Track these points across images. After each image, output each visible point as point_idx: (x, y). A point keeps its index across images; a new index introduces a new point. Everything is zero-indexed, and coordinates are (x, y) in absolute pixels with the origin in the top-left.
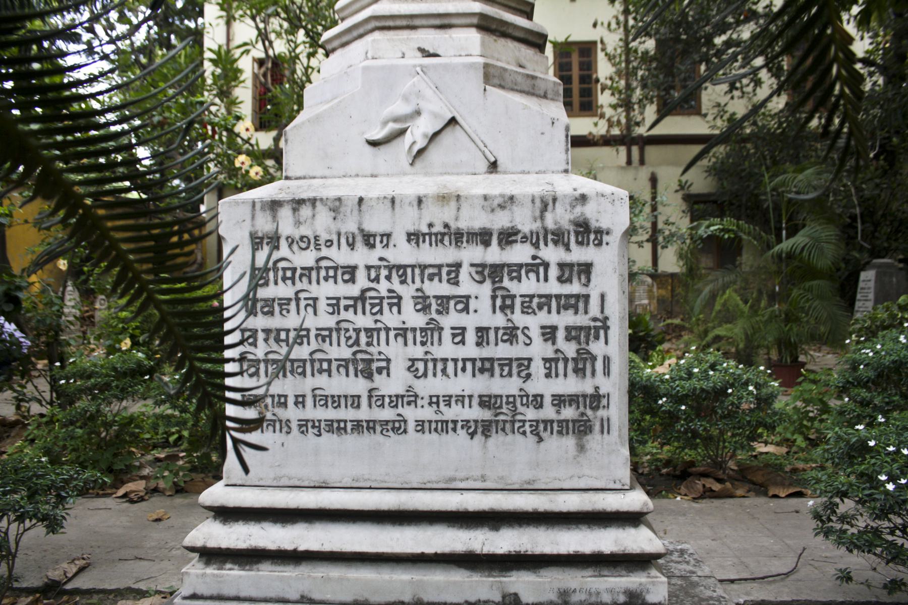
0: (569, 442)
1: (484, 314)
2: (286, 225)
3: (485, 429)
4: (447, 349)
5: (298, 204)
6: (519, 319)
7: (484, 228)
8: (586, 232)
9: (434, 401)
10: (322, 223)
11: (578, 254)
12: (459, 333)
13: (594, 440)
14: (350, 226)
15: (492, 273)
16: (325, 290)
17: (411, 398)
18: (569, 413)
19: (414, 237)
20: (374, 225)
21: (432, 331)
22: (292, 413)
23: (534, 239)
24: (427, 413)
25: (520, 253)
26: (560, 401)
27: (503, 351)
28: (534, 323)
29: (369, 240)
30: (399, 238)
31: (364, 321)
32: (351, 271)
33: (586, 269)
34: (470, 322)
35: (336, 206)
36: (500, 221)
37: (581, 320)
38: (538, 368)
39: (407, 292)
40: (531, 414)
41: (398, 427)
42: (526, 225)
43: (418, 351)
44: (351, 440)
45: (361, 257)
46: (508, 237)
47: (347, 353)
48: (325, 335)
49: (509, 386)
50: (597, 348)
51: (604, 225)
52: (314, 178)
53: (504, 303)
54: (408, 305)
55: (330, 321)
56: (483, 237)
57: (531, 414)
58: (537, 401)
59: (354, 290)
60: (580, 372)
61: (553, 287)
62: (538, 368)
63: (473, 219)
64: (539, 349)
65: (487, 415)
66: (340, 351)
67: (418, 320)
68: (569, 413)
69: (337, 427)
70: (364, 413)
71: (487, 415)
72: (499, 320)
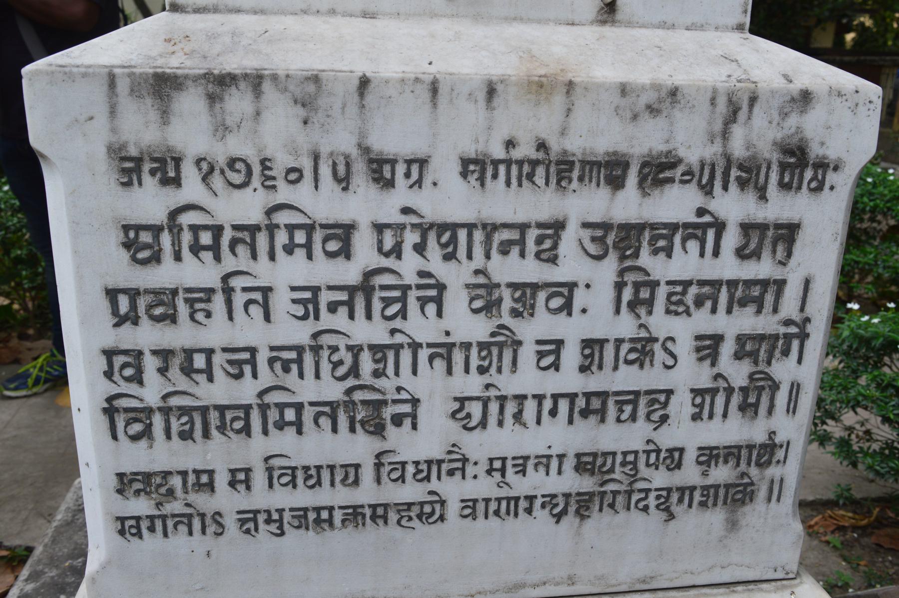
0: (716, 517)
1: (599, 314)
2: (190, 130)
3: (583, 505)
4: (527, 378)
5: (219, 84)
6: (660, 323)
7: (615, 153)
8: (800, 164)
9: (497, 467)
10: (277, 132)
11: (779, 207)
12: (551, 351)
13: (755, 514)
14: (341, 139)
15: (621, 240)
16: (288, 272)
17: (457, 464)
18: (721, 474)
19: (475, 167)
20: (391, 140)
22: (226, 500)
23: (706, 178)
24: (483, 487)
25: (676, 204)
26: (709, 456)
27: (628, 378)
28: (683, 330)
29: (381, 171)
30: (444, 168)
31: (368, 331)
32: (343, 233)
33: (788, 233)
34: (571, 330)
35: (309, 93)
36: (646, 139)
37: (766, 324)
38: (681, 406)
39: (456, 276)
40: (660, 479)
41: (430, 512)
43: (473, 385)
44: (341, 540)
45: (364, 205)
46: (658, 171)
47: (333, 391)
48: (288, 359)
50: (784, 370)
51: (832, 153)
52: (238, 11)
53: (637, 295)
54: (457, 302)
56: (611, 171)
57: (660, 479)
58: (674, 458)
59: (349, 272)
60: (748, 409)
61: (728, 267)
62: (681, 406)
63: (595, 134)
64: (689, 373)
65: (587, 484)
66: (318, 388)
67: (478, 329)
68: (721, 474)
69: (315, 519)
70: (367, 493)
71: (587, 484)
72: (626, 326)
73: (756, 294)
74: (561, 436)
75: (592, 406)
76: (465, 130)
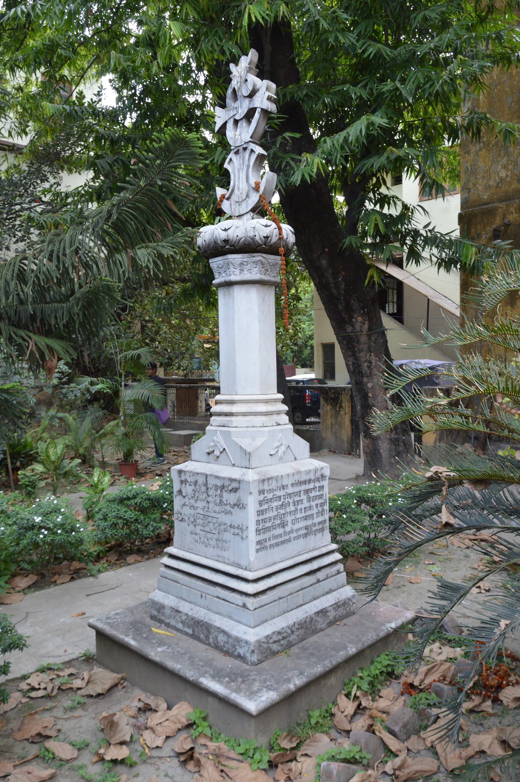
0: (320, 534)
2: (266, 487)
3: (306, 535)
8: (323, 477)
10: (274, 484)
15: (307, 491)
16: (275, 504)
20: (285, 483)
21: (296, 510)
24: (294, 535)
25: (311, 486)
27: (309, 513)
29: (284, 487)
30: (290, 486)
31: (283, 511)
32: (280, 497)
35: (276, 478)
36: (307, 478)
39: (291, 501)
41: (289, 540)
42: (313, 478)
43: (293, 517)
44: (281, 547)
45: (281, 493)
46: (310, 481)
49: (309, 522)
53: (309, 500)
54: (291, 505)
55: (275, 513)
56: (305, 482)
57: (314, 529)
58: (315, 525)
59: (280, 503)
62: (315, 516)
63: (304, 478)
66: (278, 522)
69: (277, 545)
73: (321, 497)
74: (303, 524)
75: (306, 518)
76: (291, 480)
